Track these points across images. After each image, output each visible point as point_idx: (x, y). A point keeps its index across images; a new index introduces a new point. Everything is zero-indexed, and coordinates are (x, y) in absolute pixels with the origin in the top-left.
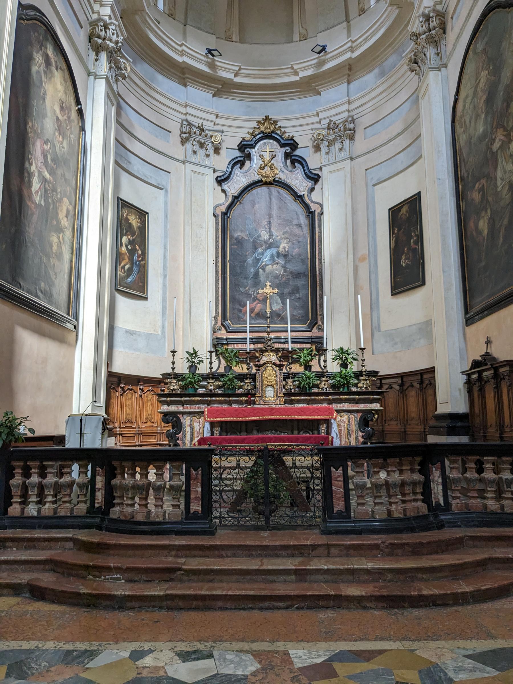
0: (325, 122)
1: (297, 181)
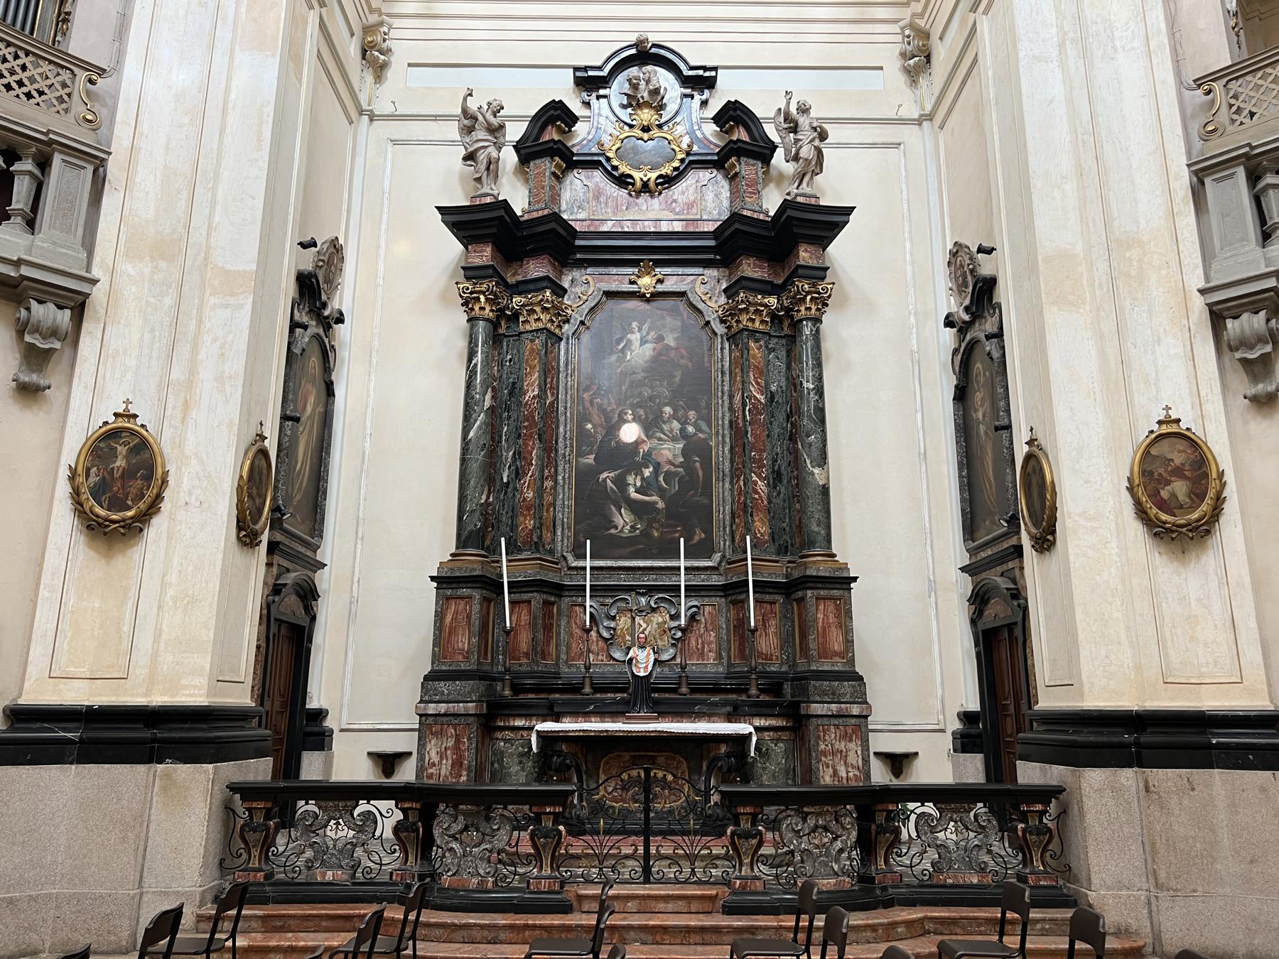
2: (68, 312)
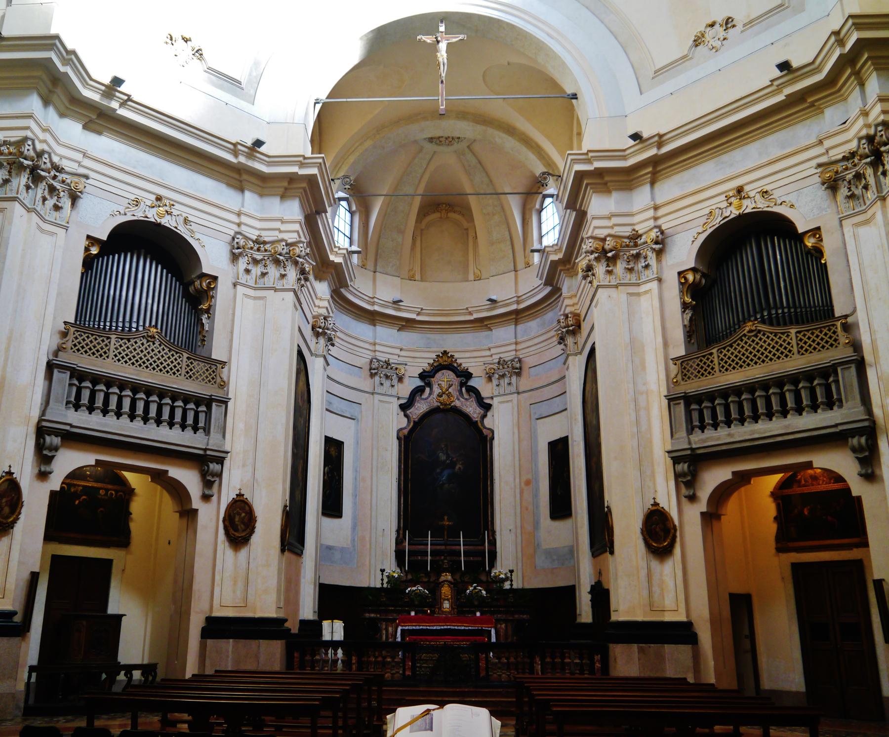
0: (496, 358)
1: (471, 408)
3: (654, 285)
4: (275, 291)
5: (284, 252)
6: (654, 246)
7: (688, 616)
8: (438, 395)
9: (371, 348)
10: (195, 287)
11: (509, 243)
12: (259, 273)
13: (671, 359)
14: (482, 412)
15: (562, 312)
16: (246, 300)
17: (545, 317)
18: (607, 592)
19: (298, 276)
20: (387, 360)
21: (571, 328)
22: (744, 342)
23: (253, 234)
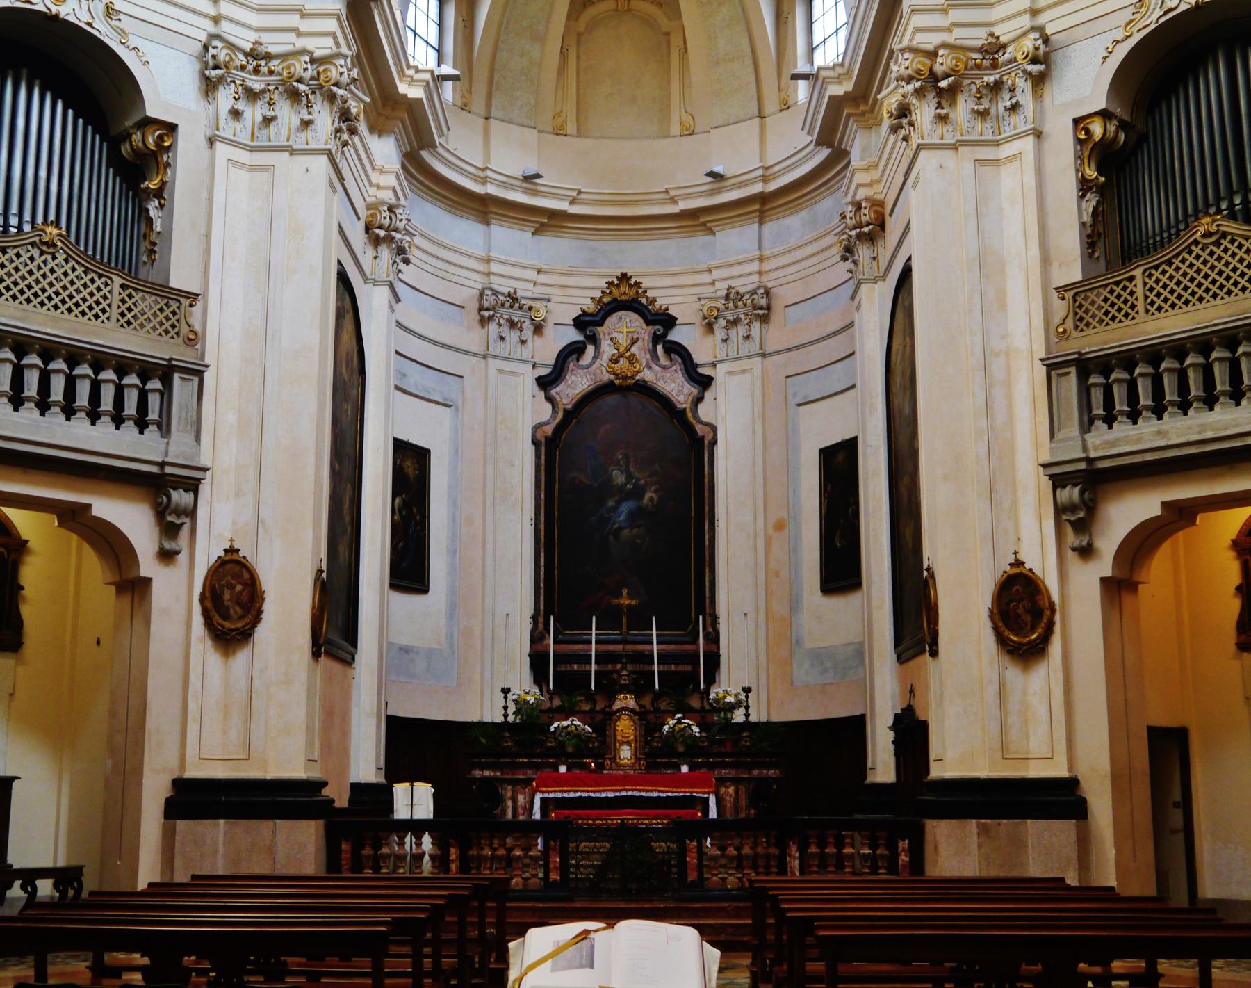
0: (721, 291)
1: (673, 385)
2: (192, 495)
3: (1028, 143)
4: (291, 154)
5: (308, 75)
6: (1030, 68)
7: (1071, 768)
8: (611, 360)
9: (481, 267)
10: (131, 146)
11: (748, 61)
12: (259, 118)
13: (1055, 289)
14: (695, 391)
15: (849, 198)
16: (237, 174)
17: (818, 207)
18: (924, 725)
19: (336, 124)
20: (512, 291)
21: (866, 230)
22: (1194, 255)
23: (245, 40)
